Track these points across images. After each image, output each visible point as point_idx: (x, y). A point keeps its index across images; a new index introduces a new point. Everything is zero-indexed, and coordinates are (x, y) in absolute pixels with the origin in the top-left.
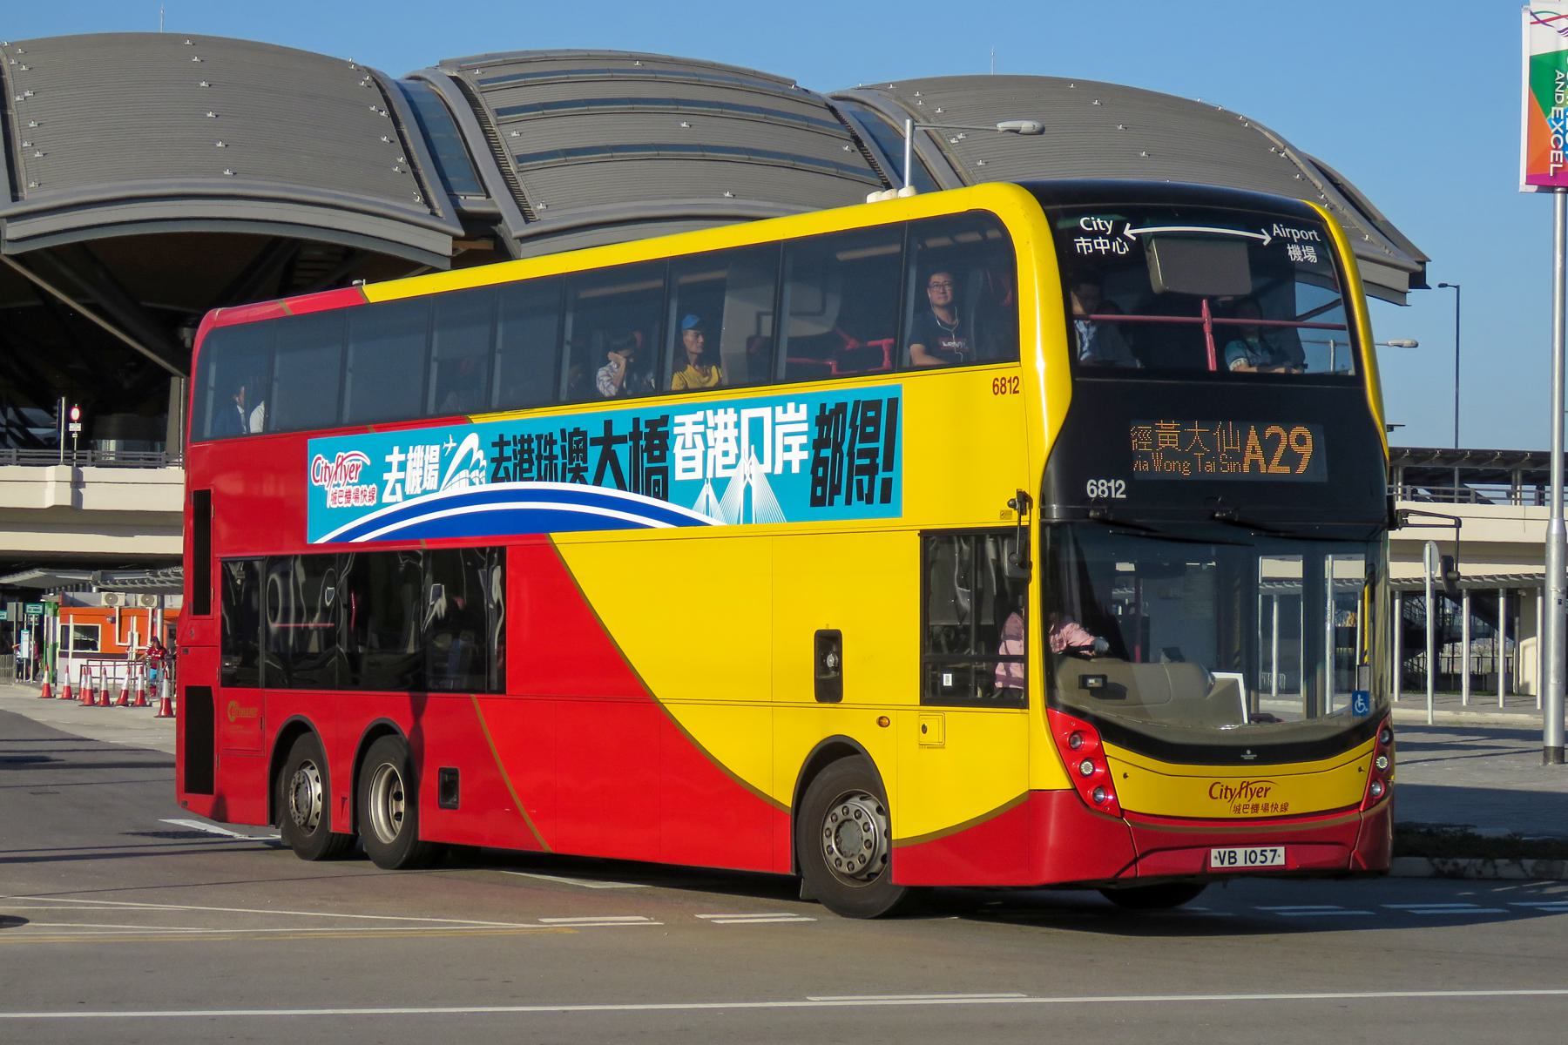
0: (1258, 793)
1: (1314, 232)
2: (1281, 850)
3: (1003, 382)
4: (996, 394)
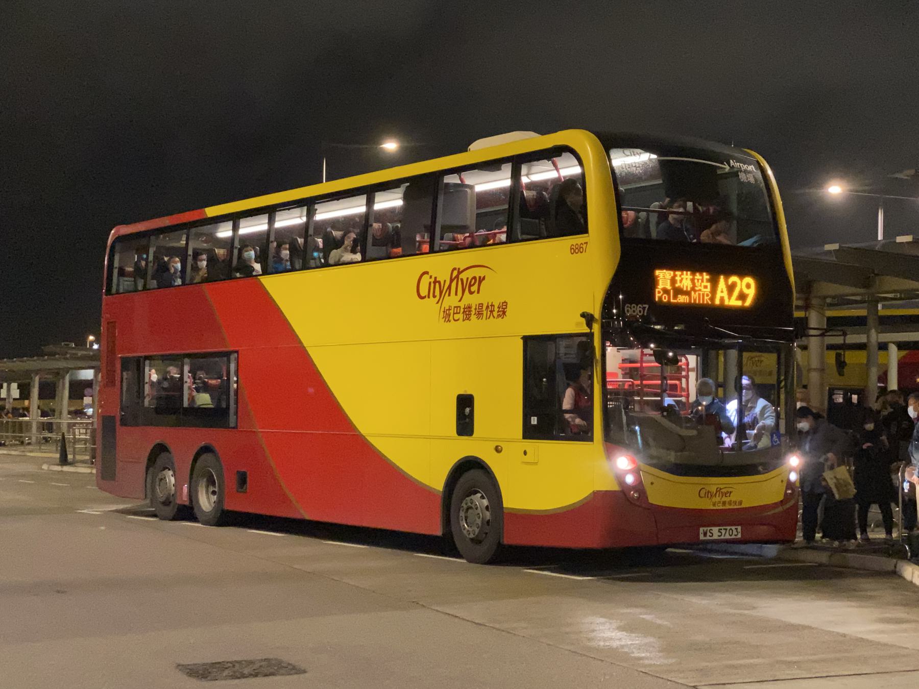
0: (726, 494)
1: (752, 166)
2: (739, 528)
3: (577, 246)
4: (572, 254)
